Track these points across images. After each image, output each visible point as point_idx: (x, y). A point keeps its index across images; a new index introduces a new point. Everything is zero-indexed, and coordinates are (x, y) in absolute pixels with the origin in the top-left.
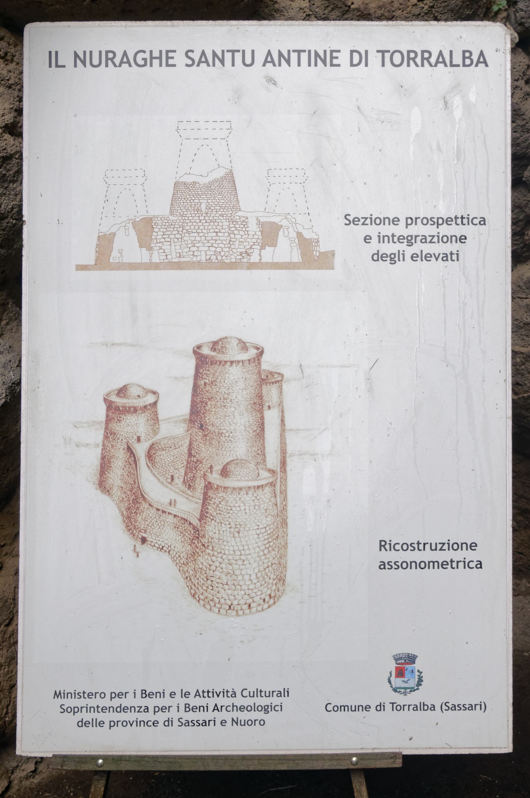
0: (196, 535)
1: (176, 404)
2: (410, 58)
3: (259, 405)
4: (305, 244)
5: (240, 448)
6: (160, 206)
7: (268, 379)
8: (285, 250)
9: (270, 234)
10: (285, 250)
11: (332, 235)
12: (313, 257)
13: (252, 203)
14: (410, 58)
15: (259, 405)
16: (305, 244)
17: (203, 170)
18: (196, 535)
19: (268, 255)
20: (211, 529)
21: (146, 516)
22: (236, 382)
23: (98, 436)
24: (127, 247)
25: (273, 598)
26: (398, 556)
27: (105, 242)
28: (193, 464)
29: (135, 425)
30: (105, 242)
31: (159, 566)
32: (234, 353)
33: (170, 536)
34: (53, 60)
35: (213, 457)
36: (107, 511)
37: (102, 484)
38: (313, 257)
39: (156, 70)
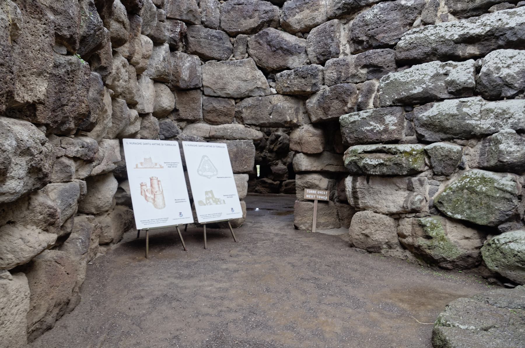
0: (154, 200)
1: (149, 185)
2: (168, 145)
3: (158, 184)
4: (160, 166)
5: (157, 189)
6: (143, 161)
7: (159, 181)
8: (158, 166)
9: (156, 164)
10: (158, 166)
11: (163, 165)
12: (161, 167)
13: (154, 161)
14: (168, 145)
15: (158, 184)
16: (160, 166)
17: (147, 157)
18: (154, 200)
19: (156, 167)
20: (156, 199)
21: (148, 198)
22: (155, 182)
23: (140, 189)
24: (139, 166)
25: (164, 207)
26: (177, 201)
27: (137, 165)
28: (152, 192)
29: (144, 187)
30: (137, 165)
31: (150, 204)
32: (154, 178)
33: (151, 200)
34: (127, 143)
35: (155, 191)
36: (143, 198)
37: (142, 194)
38: (161, 167)
39: (139, 145)
